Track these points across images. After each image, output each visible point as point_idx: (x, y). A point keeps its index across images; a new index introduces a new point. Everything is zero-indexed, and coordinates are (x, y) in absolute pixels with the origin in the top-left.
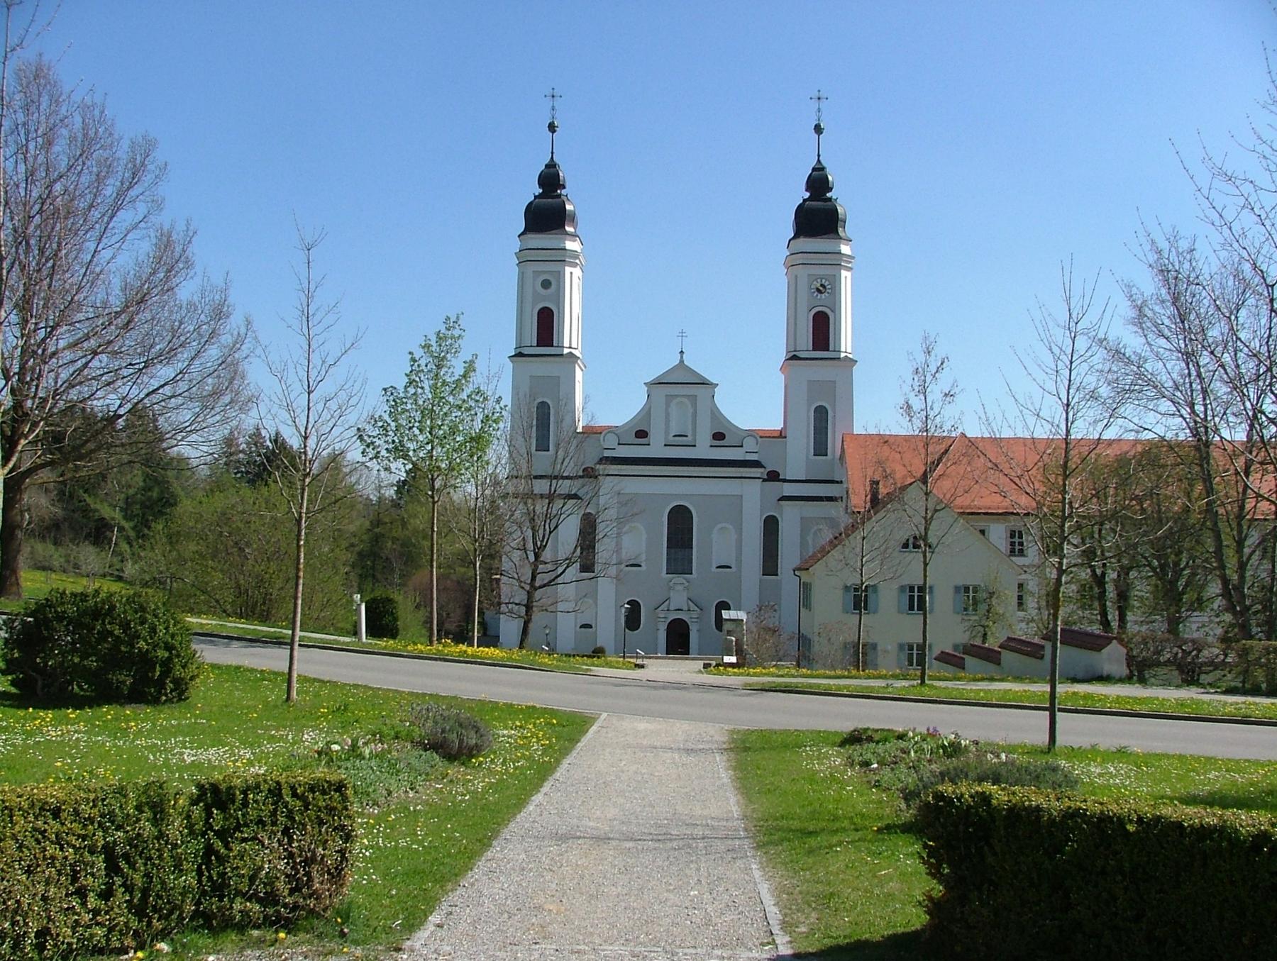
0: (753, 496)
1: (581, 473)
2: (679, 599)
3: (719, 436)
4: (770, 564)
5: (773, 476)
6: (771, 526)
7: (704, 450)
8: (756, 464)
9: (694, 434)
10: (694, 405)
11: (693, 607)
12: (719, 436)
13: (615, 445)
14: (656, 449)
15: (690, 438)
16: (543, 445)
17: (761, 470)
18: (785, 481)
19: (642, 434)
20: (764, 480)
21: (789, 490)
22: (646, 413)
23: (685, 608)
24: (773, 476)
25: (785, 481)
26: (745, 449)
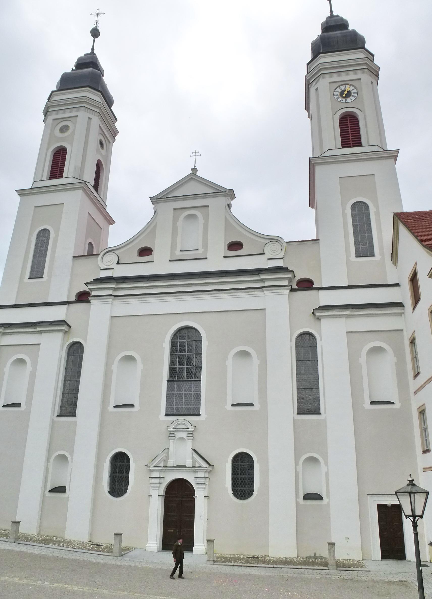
1: (73, 299)
2: (181, 453)
3: (235, 246)
4: (308, 403)
5: (306, 285)
6: (306, 345)
7: (218, 261)
9: (205, 245)
10: (206, 217)
13: (114, 265)
14: (159, 265)
15: (201, 251)
16: (37, 272)
17: (290, 275)
19: (145, 251)
20: (292, 290)
21: (326, 298)
22: (150, 228)
23: (189, 463)
24: (306, 285)
26: (268, 254)
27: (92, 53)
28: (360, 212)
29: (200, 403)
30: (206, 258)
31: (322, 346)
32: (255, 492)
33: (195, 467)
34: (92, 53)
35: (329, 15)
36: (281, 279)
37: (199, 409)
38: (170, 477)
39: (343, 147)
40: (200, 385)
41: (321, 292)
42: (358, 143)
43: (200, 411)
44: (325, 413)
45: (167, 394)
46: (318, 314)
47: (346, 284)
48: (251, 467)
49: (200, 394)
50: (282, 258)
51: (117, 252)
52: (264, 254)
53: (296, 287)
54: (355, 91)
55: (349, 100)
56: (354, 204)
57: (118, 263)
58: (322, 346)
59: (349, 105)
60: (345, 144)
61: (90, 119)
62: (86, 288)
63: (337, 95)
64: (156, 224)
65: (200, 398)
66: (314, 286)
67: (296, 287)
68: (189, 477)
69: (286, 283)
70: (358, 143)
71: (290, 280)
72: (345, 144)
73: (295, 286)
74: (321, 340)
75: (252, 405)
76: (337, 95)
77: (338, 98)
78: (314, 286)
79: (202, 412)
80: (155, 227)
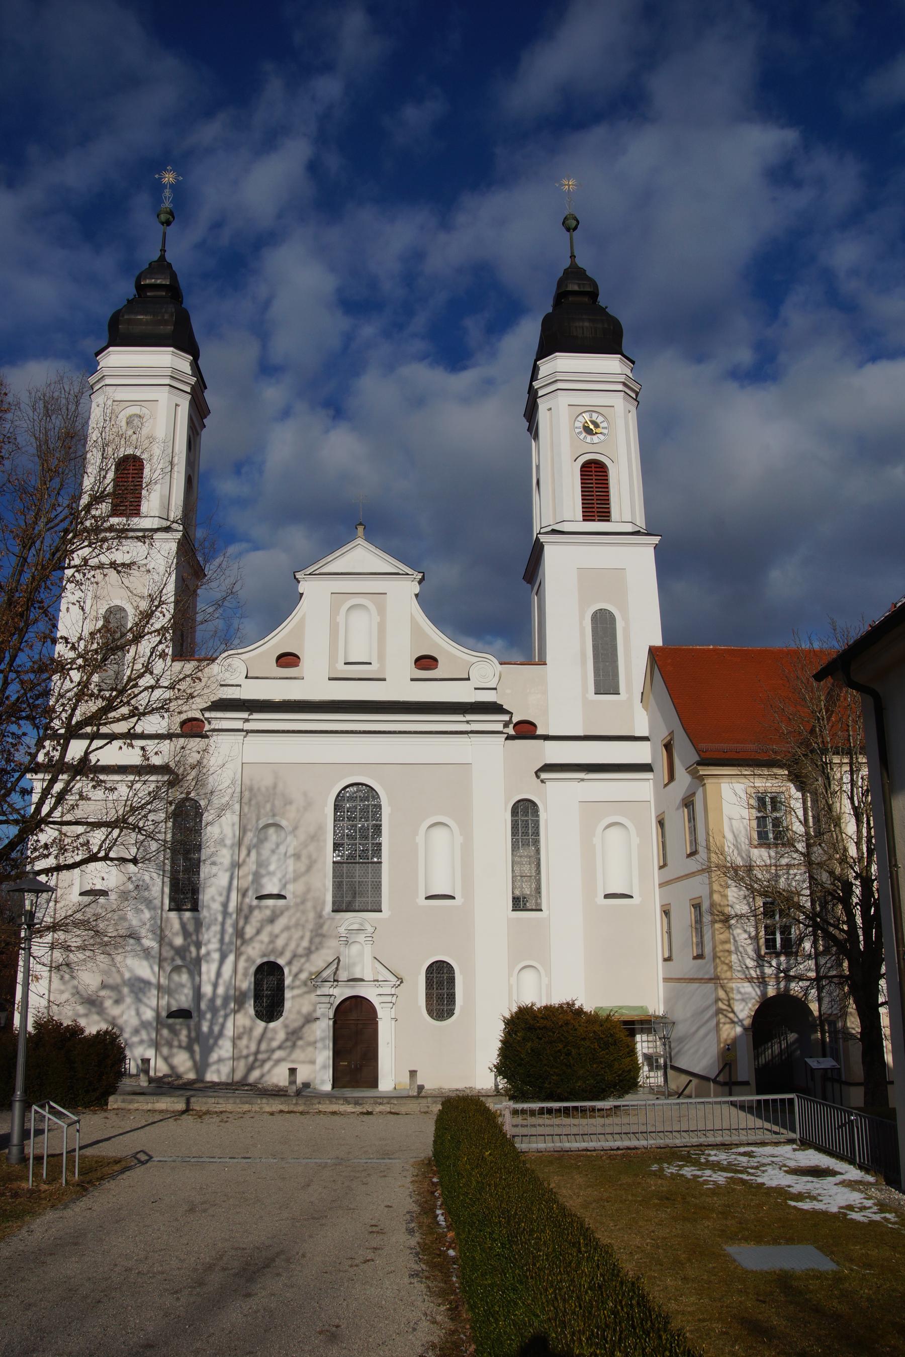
0: (490, 767)
3: (426, 662)
5: (525, 730)
7: (401, 686)
8: (494, 708)
9: (382, 657)
10: (382, 610)
11: (385, 974)
12: (426, 662)
13: (241, 680)
14: (312, 684)
17: (506, 718)
18: (546, 738)
19: (288, 659)
23: (368, 976)
24: (525, 730)
25: (546, 738)
26: (475, 682)
27: (162, 258)
28: (604, 627)
29: (380, 894)
30: (384, 680)
31: (546, 821)
32: (457, 1011)
33: (377, 981)
34: (162, 258)
35: (567, 263)
36: (494, 722)
37: (379, 903)
38: (341, 993)
39: (584, 520)
40: (380, 870)
41: (548, 743)
42: (605, 516)
43: (380, 906)
44: (549, 909)
45: (334, 882)
46: (543, 776)
47: (581, 734)
48: (452, 981)
49: (380, 882)
50: (495, 689)
51: (244, 657)
52: (468, 679)
53: (514, 733)
54: (605, 425)
55: (595, 439)
56: (596, 612)
57: (246, 677)
58: (546, 821)
59: (593, 447)
60: (588, 516)
61: (177, 405)
62: (198, 715)
63: (579, 428)
64: (304, 615)
65: (380, 888)
66: (539, 732)
67: (514, 733)
68: (369, 993)
69: (499, 727)
70: (605, 516)
71: (506, 725)
72: (588, 516)
73: (511, 731)
74: (546, 810)
75: (454, 898)
76: (579, 428)
77: (580, 433)
78: (539, 732)
79: (384, 907)
80: (303, 619)
